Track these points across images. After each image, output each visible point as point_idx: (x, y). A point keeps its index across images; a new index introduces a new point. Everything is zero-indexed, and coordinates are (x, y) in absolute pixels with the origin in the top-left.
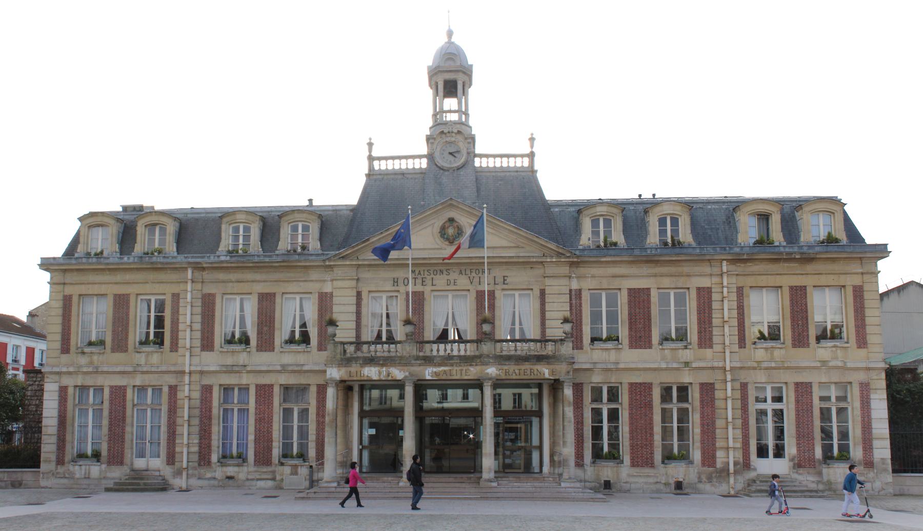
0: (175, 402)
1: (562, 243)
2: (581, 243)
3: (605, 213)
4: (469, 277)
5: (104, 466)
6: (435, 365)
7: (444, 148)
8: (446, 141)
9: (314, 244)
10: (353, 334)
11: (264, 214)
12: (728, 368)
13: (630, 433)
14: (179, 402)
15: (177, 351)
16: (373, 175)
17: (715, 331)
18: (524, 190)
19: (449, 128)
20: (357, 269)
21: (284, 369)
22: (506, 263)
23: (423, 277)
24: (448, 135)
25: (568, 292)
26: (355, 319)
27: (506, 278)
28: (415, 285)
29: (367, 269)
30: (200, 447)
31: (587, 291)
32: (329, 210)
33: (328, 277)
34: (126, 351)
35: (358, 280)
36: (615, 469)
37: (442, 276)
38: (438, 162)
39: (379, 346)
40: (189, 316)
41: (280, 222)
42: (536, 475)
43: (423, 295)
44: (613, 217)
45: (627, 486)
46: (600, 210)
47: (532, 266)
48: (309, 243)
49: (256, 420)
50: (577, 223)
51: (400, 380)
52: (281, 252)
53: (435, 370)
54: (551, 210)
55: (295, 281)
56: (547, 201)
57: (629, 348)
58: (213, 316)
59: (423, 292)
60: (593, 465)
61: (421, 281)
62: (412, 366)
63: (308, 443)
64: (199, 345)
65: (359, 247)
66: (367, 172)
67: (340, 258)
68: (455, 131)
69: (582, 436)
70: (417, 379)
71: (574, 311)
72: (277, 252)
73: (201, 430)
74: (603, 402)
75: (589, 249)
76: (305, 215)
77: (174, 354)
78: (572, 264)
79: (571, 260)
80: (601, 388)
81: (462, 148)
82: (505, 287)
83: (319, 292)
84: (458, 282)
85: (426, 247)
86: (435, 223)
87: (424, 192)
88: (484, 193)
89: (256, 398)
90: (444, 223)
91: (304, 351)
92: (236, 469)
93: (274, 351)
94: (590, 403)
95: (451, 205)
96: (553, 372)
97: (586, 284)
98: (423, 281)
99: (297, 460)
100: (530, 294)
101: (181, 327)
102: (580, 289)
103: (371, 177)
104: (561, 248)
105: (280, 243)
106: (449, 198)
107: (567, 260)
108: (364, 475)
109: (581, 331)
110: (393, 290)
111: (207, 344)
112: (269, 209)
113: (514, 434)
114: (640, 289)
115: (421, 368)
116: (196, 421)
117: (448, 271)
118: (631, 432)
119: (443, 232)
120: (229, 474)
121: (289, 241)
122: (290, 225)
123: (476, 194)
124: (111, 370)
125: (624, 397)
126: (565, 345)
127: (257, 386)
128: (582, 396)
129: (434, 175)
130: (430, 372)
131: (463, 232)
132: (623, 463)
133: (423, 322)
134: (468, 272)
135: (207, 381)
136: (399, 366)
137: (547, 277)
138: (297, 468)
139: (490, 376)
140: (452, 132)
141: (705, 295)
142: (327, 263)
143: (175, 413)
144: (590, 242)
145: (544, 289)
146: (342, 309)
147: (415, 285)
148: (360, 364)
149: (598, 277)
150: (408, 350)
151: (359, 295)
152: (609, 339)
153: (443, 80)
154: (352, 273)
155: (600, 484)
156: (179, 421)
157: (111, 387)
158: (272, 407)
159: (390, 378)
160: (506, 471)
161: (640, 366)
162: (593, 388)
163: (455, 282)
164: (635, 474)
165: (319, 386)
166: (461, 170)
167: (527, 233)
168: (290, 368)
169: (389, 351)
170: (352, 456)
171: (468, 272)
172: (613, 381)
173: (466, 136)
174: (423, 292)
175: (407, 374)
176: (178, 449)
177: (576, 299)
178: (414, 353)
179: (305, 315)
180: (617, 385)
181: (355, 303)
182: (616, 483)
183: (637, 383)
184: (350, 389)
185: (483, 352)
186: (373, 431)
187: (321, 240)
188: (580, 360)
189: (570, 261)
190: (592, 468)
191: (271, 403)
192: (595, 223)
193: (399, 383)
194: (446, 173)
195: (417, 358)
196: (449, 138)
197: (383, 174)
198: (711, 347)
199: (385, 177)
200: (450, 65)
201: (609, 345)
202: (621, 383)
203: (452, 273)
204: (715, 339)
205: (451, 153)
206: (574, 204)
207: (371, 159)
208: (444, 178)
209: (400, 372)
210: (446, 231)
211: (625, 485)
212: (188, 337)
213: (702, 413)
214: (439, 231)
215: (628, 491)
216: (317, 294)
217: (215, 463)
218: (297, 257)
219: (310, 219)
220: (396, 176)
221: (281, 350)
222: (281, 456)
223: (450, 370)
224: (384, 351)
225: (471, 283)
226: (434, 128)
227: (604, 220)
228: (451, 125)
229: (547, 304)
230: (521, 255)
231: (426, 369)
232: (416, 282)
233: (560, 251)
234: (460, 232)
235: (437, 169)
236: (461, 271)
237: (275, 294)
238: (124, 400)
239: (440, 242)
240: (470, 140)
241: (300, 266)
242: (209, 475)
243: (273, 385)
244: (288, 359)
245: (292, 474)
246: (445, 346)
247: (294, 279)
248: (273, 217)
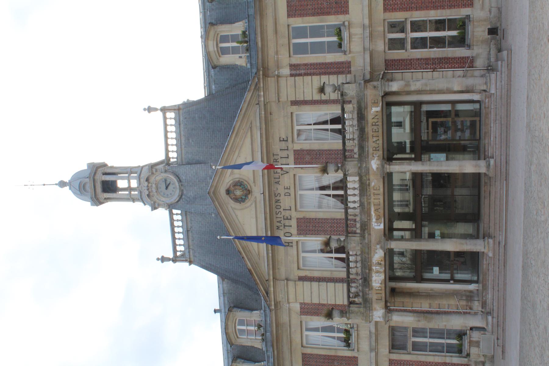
1: (245, 84)
2: (244, 65)
3: (215, 42)
4: (282, 175)
6: (370, 220)
7: (162, 194)
8: (156, 192)
9: (256, 316)
10: (339, 285)
11: (230, 360)
13: (437, 9)
16: (190, 258)
18: (197, 118)
19: (145, 190)
20: (278, 280)
21: (374, 349)
22: (267, 139)
23: (283, 218)
24: (150, 190)
25: (293, 78)
26: (325, 283)
27: (282, 139)
28: (291, 226)
29: (277, 271)
31: (291, 58)
32: (224, 300)
33: (286, 306)
35: (287, 279)
36: (475, 23)
37: (281, 201)
38: (175, 200)
39: (351, 259)
41: (237, 345)
42: (483, 107)
43: (300, 219)
44: (218, 34)
45: (494, 10)
46: (212, 47)
47: (269, 113)
48: (255, 320)
50: (225, 68)
51: (385, 254)
52: (264, 346)
53: (374, 220)
54: (214, 92)
55: (290, 335)
56: (205, 96)
57: (348, 14)
59: (297, 219)
60: (472, 47)
61: (287, 220)
62: (370, 242)
63: (446, 329)
65: (257, 278)
66: (187, 264)
67: (268, 296)
68: (146, 184)
69: (441, 59)
70: (383, 237)
71: (312, 71)
72: (264, 349)
74: (404, 37)
75: (250, 57)
76: (229, 323)
78: (266, 75)
79: (261, 77)
80: (391, 40)
81: (161, 177)
82: (290, 139)
83: (301, 315)
84: (287, 185)
85: (254, 216)
86: (231, 207)
87: (203, 214)
88: (201, 157)
90: (231, 199)
91: (357, 330)
93: (357, 358)
94: (406, 51)
95: (214, 193)
96: (375, 103)
97: (285, 59)
98: (287, 219)
99: (465, 341)
100: (297, 115)
102: (290, 66)
103: (192, 259)
104: (250, 87)
105: (255, 346)
106: (208, 195)
107: (261, 81)
108: (481, 278)
109: (331, 64)
110: (296, 247)
112: (226, 352)
113: (439, 129)
114: (287, 5)
115: (372, 233)
117: (276, 195)
118: (435, 8)
119: (239, 200)
121: (254, 337)
122: (239, 336)
123: (203, 165)
125: (398, 16)
126: (346, 92)
128: (399, 60)
129: (187, 204)
130: (376, 224)
131: (239, 181)
132: (469, 15)
133: (327, 219)
134: (277, 176)
136: (371, 253)
137: (278, 99)
138: (472, 341)
139: (380, 166)
140: (148, 186)
142: (273, 307)
144: (243, 55)
145: (291, 101)
146: (315, 294)
147: (291, 226)
148: (369, 290)
149: (277, 47)
150: (355, 245)
151: (302, 279)
152: (339, 34)
153: (102, 194)
154: (281, 285)
155: (491, 40)
158: (411, 361)
159: (383, 263)
160: (478, 137)
162: (389, 49)
163: (287, 189)
164: (481, 2)
166: (181, 178)
167: (237, 121)
168: (373, 344)
169: (356, 262)
170: (460, 290)
171: (277, 176)
172: (383, 29)
173: (150, 174)
174: (297, 219)
175: (378, 246)
177: (300, 69)
178: (357, 238)
179: (321, 326)
180: (386, 24)
181: (309, 283)
182: (491, 22)
183: (384, 4)
184: (393, 291)
185: (356, 173)
186: (436, 270)
187: (251, 309)
188: (362, 64)
189: (263, 77)
190: (475, 48)
192: (224, 51)
193: (387, 254)
194: (185, 192)
195: (363, 236)
196: (153, 189)
197: (189, 248)
199: (191, 247)
200: (89, 187)
201: (345, 35)
202: (384, 20)
203: (279, 191)
205: (167, 188)
206: (207, 71)
207: (175, 260)
208: (189, 194)
209: (377, 253)
210: (238, 197)
211: (492, 14)
214: (239, 204)
215: (499, 10)
216: (301, 316)
218: (268, 334)
219: (233, 319)
220: (190, 237)
221: (356, 350)
222: (460, 355)
223: (374, 205)
224: (356, 267)
225: (287, 172)
226: (145, 202)
227: (221, 42)
228: (141, 187)
229: (305, 99)
230: (258, 124)
231: (374, 228)
232: (287, 225)
233: (253, 87)
234: (239, 184)
235: (181, 200)
236: (276, 183)
237: (303, 354)
239: (249, 202)
240: (154, 170)
241: (276, 332)
243: (390, 360)
244: (365, 345)
245: (478, 346)
246: (350, 195)
247: (289, 337)
248: (233, 349)
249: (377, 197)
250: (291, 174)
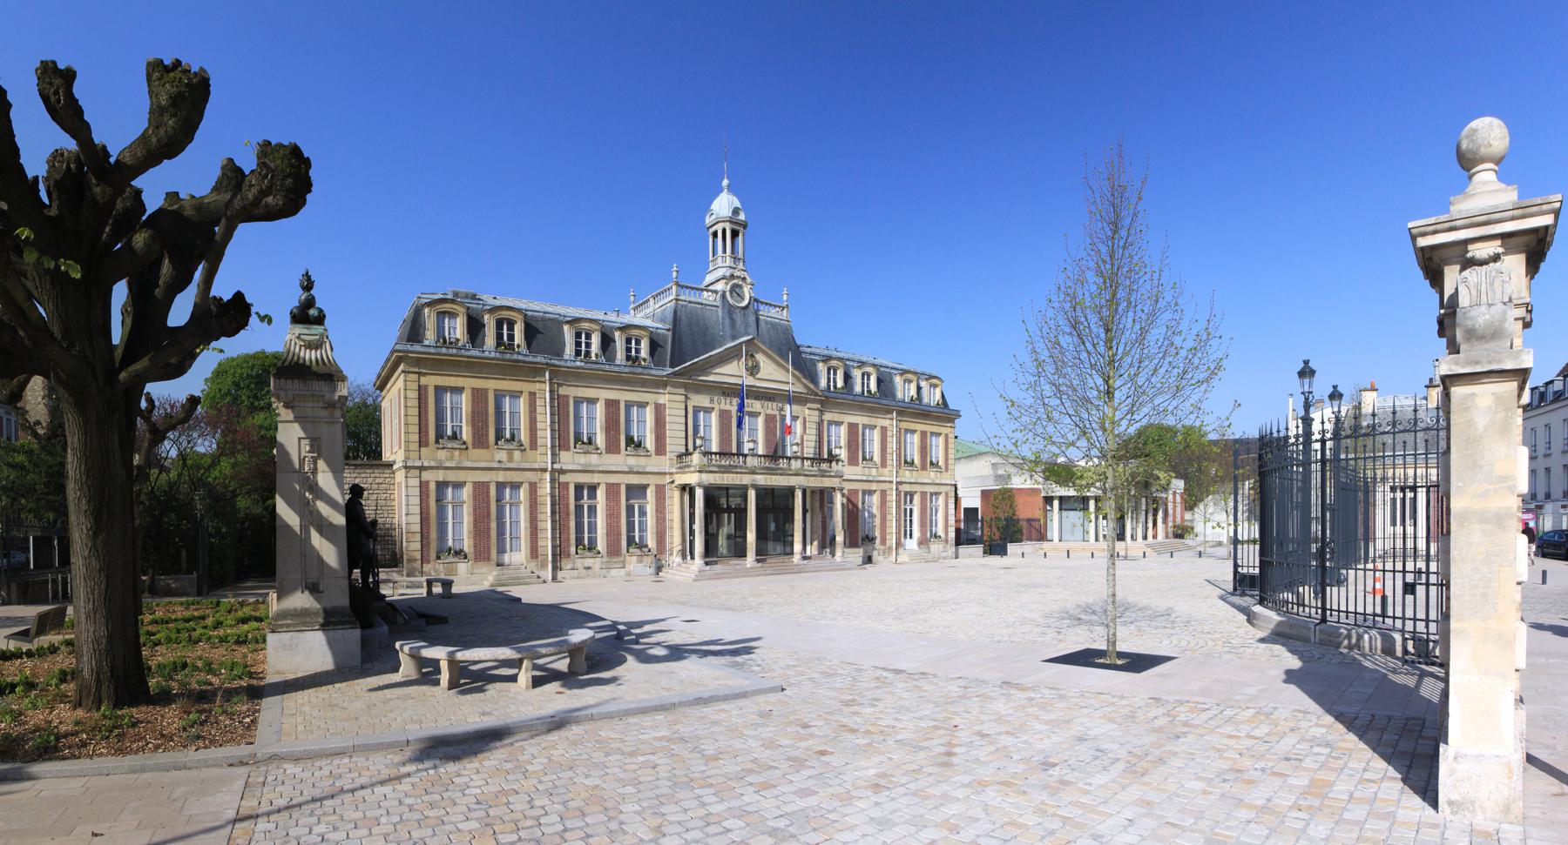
0: (536, 499)
34: (487, 448)
92: (592, 560)
120: (586, 565)
124: (475, 465)
156: (540, 517)
157: (474, 483)
161: (854, 478)
165: (657, 486)
242: (569, 566)
244: (632, 461)
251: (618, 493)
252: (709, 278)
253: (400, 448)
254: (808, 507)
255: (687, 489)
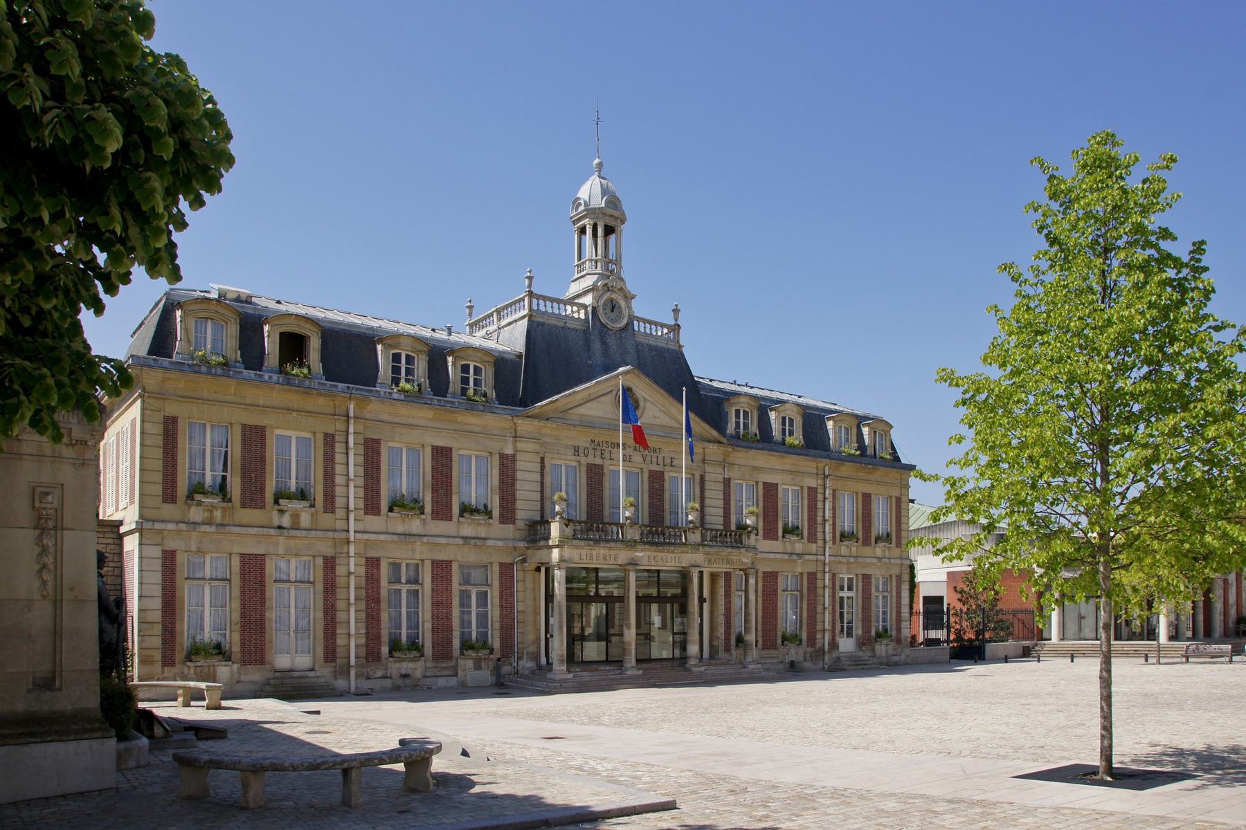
0: (333, 579)
5: (235, 666)
12: (827, 561)
14: (341, 581)
15: (333, 512)
17: (819, 529)
30: (367, 638)
40: (351, 466)
43: (603, 470)
49: (433, 604)
58: (378, 469)
59: (602, 466)
64: (362, 506)
73: (367, 616)
77: (330, 515)
89: (433, 578)
101: (339, 480)
111: (371, 507)
116: (363, 605)
118: (763, 618)
127: (433, 562)
135: (372, 554)
141: (812, 492)
143: (334, 594)
151: (542, 459)
156: (341, 605)
165: (501, 564)
174: (602, 466)
176: (340, 641)
191: (449, 583)
194: (610, 332)
198: (816, 542)
204: (820, 535)
212: (352, 494)
213: (808, 601)
217: (387, 659)
238: (263, 575)
243: (451, 562)
244: (467, 530)
249: (673, 559)
250: (643, 466)
251: (449, 574)
252: (574, 288)
253: (132, 502)
254: (706, 594)
255: (543, 569)
